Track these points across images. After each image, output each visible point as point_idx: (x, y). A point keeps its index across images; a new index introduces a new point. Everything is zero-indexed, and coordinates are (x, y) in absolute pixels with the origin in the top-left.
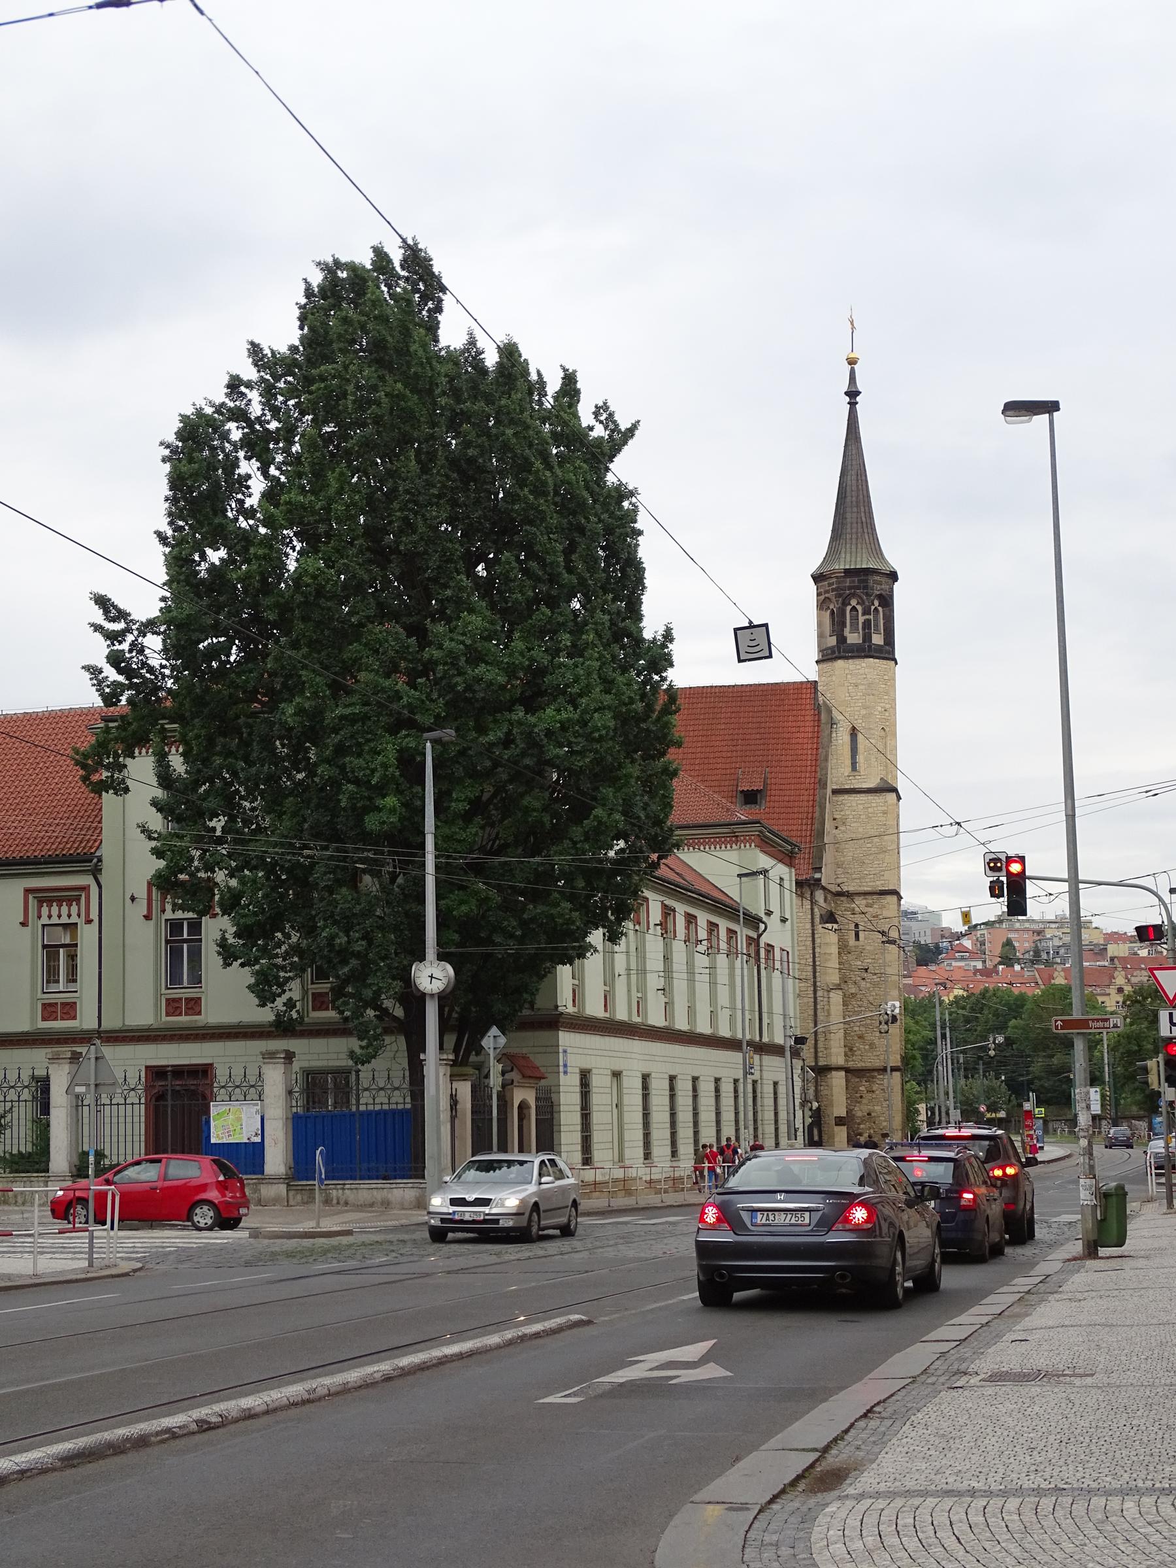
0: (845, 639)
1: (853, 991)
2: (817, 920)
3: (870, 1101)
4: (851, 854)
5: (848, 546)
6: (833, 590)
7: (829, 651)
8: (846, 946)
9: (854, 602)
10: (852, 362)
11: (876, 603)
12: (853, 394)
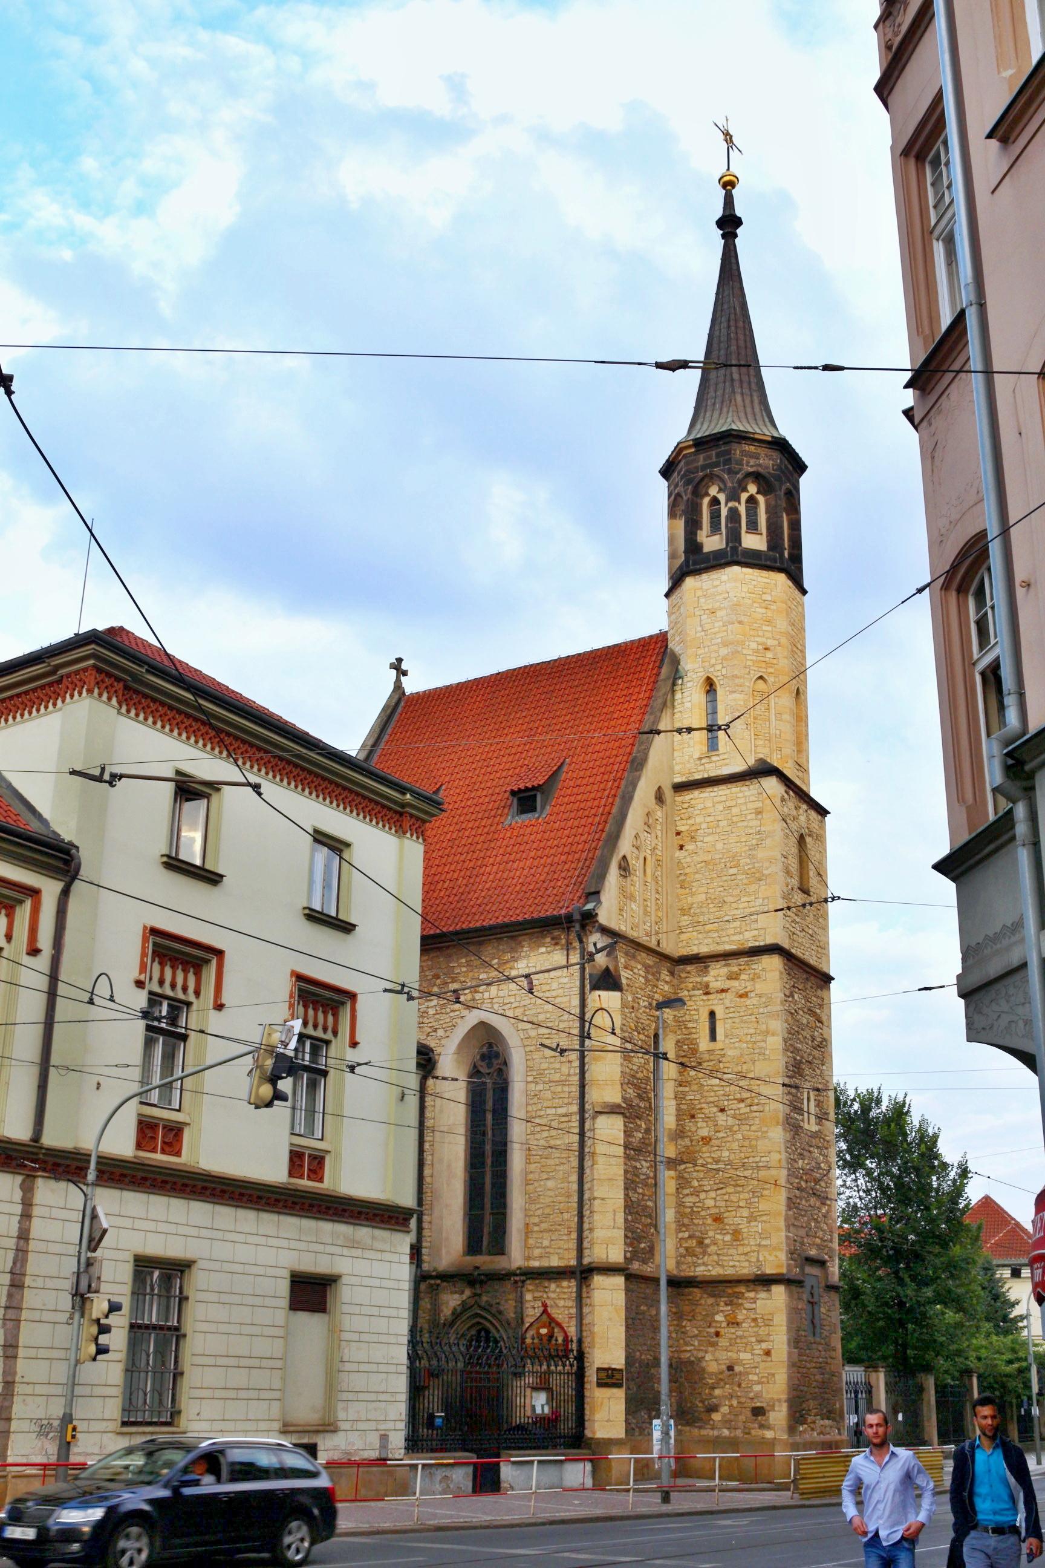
1: (704, 1132)
2: (588, 987)
3: (732, 1343)
4: (703, 889)
5: (708, 414)
8: (694, 1051)
9: (713, 491)
11: (752, 489)
12: (729, 223)
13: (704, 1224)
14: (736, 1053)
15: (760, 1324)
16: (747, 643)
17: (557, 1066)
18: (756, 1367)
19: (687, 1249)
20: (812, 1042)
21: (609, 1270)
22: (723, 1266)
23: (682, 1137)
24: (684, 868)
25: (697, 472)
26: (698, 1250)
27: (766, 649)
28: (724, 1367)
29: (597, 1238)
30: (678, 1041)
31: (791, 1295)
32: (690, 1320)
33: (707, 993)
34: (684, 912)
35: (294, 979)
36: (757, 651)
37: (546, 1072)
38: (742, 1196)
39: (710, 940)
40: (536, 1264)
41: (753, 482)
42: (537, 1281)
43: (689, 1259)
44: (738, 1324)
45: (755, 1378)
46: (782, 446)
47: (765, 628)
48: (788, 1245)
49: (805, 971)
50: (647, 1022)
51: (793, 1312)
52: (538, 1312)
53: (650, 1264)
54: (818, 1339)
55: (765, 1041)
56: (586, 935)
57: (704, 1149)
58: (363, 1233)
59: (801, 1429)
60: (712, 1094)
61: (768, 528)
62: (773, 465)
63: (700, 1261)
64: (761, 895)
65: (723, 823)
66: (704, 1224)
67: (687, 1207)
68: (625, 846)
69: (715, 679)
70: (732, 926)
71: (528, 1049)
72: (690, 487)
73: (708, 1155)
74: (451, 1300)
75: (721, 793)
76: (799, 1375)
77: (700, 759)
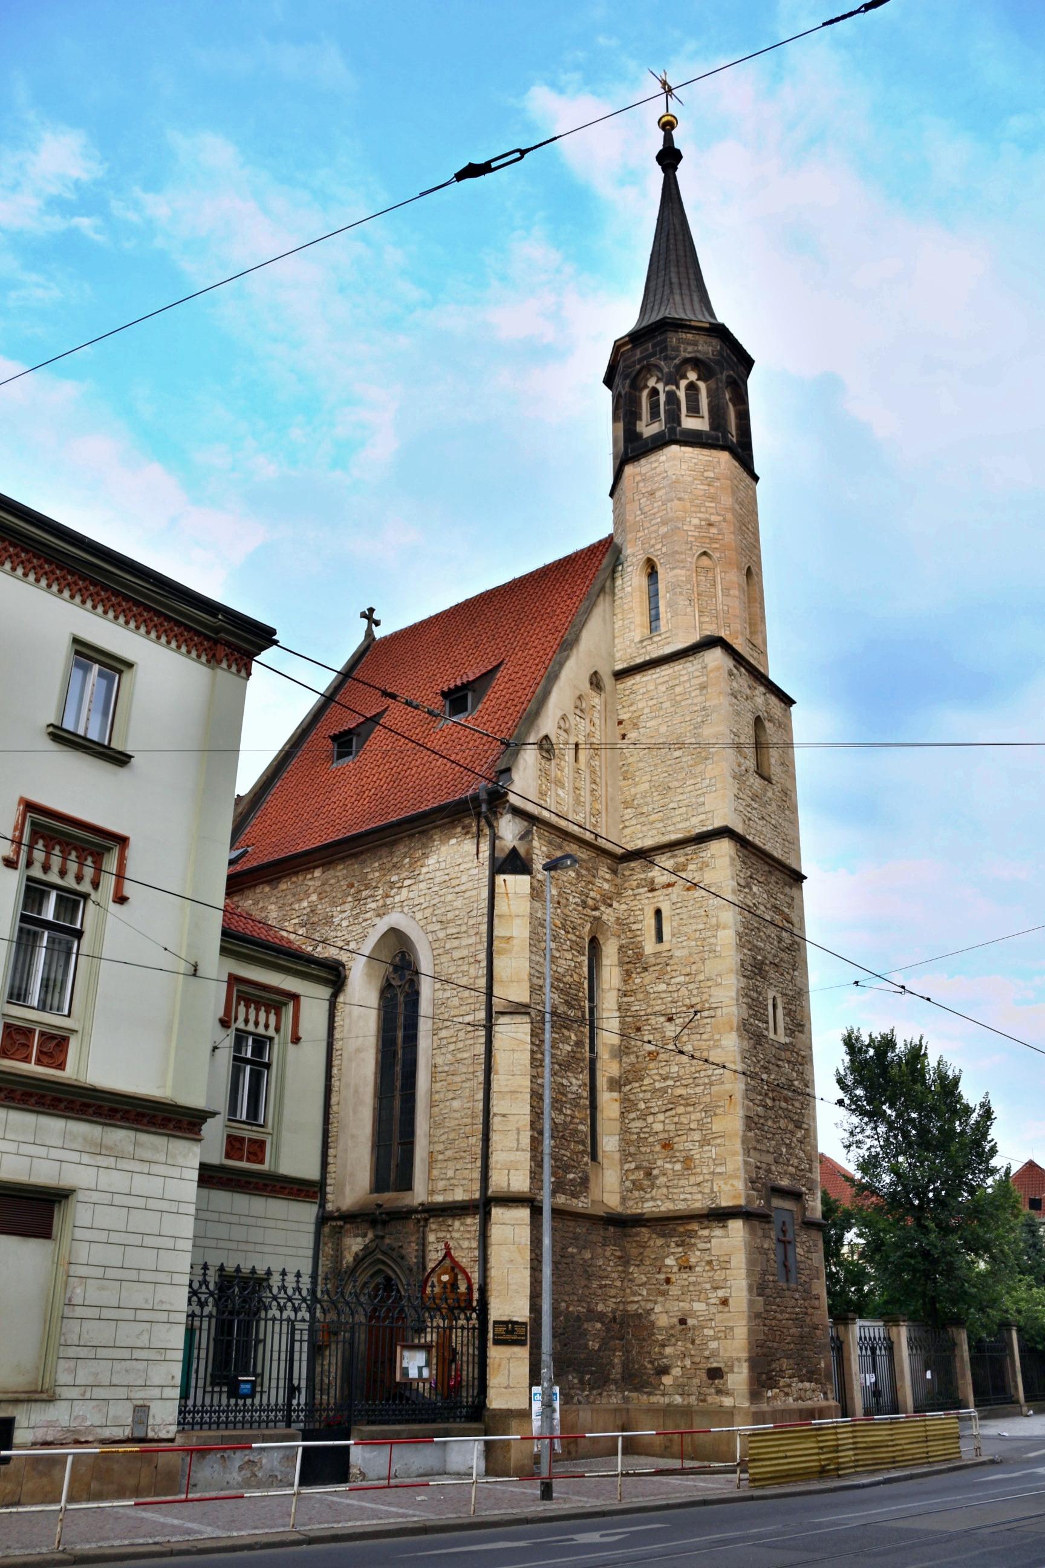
4: (647, 777)
8: (639, 955)
9: (652, 383)
10: (668, 126)
11: (692, 376)
12: (669, 158)
13: (652, 1151)
14: (685, 952)
15: (715, 1268)
16: (688, 519)
17: (465, 968)
18: (711, 1320)
19: (633, 1182)
20: (779, 942)
21: (510, 1200)
22: (673, 1200)
23: (627, 1054)
24: (627, 758)
25: (635, 366)
26: (646, 1182)
27: (710, 525)
28: (675, 1320)
29: (497, 1162)
30: (621, 947)
31: (752, 1232)
32: (638, 1266)
33: (652, 890)
34: (627, 805)
35: (21, 807)
36: (700, 527)
37: (454, 976)
38: (693, 1117)
39: (655, 832)
40: (439, 1198)
41: (692, 370)
42: (441, 1219)
43: (636, 1194)
44: (690, 1268)
45: (711, 1333)
46: (721, 332)
47: (707, 504)
48: (746, 1171)
49: (766, 862)
50: (579, 921)
51: (755, 1254)
52: (441, 1255)
53: (582, 1199)
54: (793, 1285)
55: (715, 936)
56: (497, 819)
57: (652, 1065)
58: (120, 1137)
59: (770, 1394)
60: (659, 1002)
61: (710, 411)
62: (713, 351)
63: (648, 1196)
64: (707, 776)
65: (667, 704)
66: (652, 1151)
67: (633, 1133)
68: (548, 724)
69: (655, 559)
70: (677, 813)
71: (435, 953)
72: (628, 381)
73: (655, 1071)
74: (354, 1245)
75: (663, 673)
76: (766, 1328)
77: (642, 641)
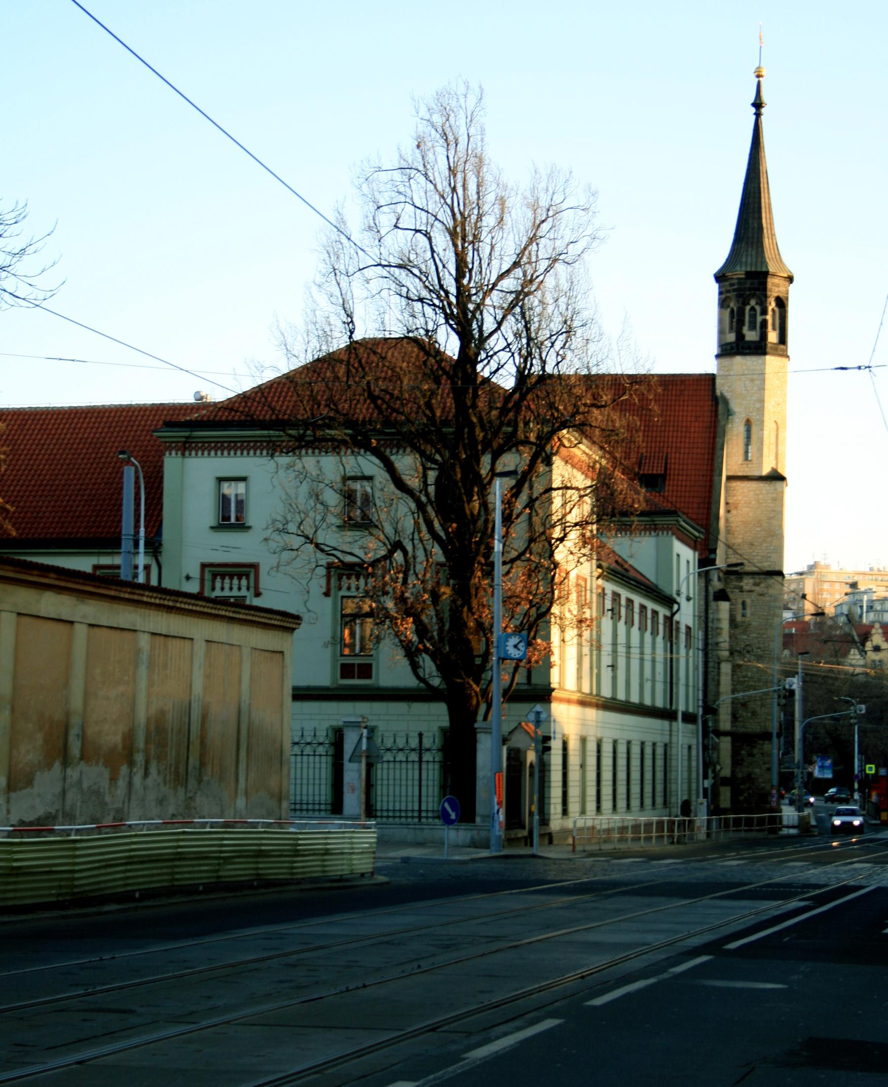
0: (743, 336)
2: (711, 597)
6: (734, 290)
7: (729, 347)
9: (753, 302)
12: (758, 105)
21: (726, 734)
33: (742, 591)
